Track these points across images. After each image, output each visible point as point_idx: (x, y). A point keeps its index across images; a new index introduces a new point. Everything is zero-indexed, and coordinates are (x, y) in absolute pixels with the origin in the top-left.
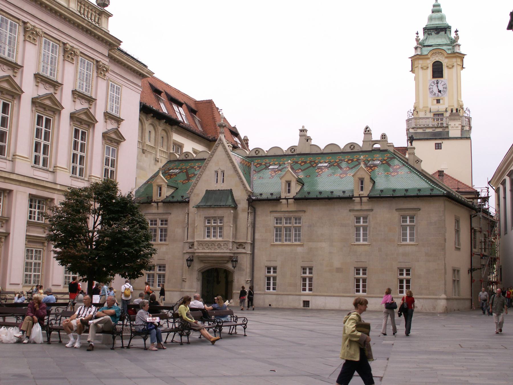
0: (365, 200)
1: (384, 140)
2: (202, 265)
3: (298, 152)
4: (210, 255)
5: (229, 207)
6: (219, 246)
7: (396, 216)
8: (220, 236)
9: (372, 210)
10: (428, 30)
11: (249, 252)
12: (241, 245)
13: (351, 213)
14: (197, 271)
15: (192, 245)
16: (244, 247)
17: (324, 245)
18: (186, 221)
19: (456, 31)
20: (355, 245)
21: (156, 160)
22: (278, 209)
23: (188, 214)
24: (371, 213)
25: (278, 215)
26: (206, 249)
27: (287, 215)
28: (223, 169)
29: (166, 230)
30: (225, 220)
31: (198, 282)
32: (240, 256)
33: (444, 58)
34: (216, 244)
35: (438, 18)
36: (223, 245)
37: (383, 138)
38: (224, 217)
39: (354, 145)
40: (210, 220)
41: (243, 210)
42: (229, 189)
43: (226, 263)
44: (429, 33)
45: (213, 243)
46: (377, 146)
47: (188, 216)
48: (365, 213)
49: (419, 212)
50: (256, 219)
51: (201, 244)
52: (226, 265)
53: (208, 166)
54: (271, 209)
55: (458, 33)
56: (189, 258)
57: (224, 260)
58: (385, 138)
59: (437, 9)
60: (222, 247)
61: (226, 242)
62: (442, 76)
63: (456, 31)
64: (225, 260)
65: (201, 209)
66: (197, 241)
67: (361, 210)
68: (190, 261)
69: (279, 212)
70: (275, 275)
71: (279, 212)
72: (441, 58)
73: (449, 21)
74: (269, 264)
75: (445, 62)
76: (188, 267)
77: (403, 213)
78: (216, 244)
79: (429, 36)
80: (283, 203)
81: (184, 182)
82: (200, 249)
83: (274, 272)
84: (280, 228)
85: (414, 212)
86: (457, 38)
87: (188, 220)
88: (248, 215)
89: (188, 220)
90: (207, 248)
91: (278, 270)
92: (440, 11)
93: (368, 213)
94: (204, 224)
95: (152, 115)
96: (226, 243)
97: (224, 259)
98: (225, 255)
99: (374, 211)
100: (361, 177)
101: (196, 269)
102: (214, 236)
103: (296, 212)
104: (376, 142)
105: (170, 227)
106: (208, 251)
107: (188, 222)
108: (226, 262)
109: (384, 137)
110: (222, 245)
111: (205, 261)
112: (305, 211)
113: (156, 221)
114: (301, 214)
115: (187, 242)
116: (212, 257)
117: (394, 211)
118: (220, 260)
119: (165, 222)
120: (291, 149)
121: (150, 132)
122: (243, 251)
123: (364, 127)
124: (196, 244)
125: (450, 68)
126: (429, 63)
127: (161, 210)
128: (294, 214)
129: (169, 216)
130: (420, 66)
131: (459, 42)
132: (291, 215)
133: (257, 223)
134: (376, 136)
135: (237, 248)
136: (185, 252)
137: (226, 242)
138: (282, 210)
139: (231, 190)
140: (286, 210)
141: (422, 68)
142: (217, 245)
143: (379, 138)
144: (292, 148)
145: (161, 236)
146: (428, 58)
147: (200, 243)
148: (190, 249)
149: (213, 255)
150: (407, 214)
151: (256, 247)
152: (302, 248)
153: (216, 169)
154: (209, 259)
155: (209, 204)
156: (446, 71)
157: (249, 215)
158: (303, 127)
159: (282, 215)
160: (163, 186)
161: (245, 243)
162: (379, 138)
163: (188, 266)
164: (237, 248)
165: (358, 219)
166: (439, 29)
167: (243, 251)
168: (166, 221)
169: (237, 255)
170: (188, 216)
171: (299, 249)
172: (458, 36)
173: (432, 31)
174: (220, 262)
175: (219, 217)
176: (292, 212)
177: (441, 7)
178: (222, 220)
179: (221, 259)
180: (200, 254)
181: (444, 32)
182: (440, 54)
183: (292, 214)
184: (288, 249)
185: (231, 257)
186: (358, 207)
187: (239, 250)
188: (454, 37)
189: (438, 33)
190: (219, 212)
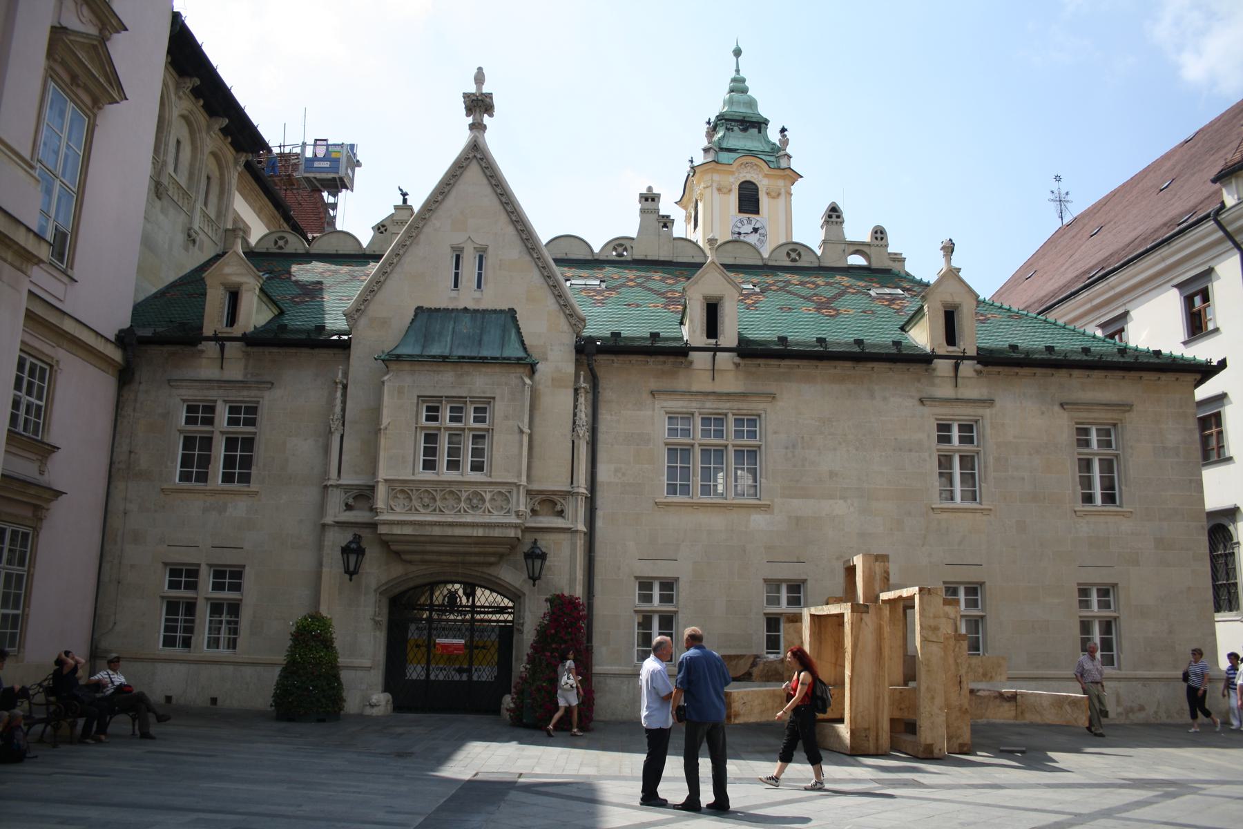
0: (967, 368)
1: (879, 242)
2: (397, 570)
3: (638, 254)
4: (437, 531)
5: (519, 362)
6: (476, 500)
7: (1062, 426)
8: (477, 467)
9: (989, 402)
10: (726, 120)
11: (581, 527)
12: (549, 502)
13: (926, 410)
14: (375, 591)
15: (364, 495)
16: (559, 508)
17: (839, 507)
18: (338, 409)
19: (783, 130)
20: (943, 510)
21: (189, 236)
22: (681, 384)
23: (345, 387)
24: (987, 412)
25: (677, 405)
26: (422, 510)
27: (710, 406)
28: (481, 240)
29: (249, 443)
30: (500, 408)
31: (378, 633)
32: (545, 542)
33: (760, 176)
34: (464, 496)
35: (744, 103)
36: (492, 499)
37: (876, 238)
38: (494, 398)
39: (800, 249)
40: (436, 409)
41: (557, 382)
42: (505, 307)
43: (491, 564)
44: (729, 126)
45: (451, 491)
46: (856, 260)
47: (344, 395)
48: (965, 413)
49: (1127, 415)
50: (600, 417)
51: (403, 491)
52: (493, 571)
53: (426, 230)
54: (653, 384)
55: (786, 133)
56: (350, 542)
57: (485, 554)
58: (882, 239)
59: (738, 86)
60: (487, 505)
61: (504, 489)
62: (757, 212)
63: (783, 130)
64: (494, 554)
65: (407, 367)
66: (386, 481)
67: (957, 400)
68: (353, 551)
69: (684, 393)
70: (668, 608)
71: (684, 393)
72: (756, 177)
73: (763, 111)
74: (648, 570)
75: (763, 184)
76: (347, 576)
77: (1083, 415)
78: (464, 496)
79: (727, 133)
80: (696, 365)
81: (297, 300)
82: (398, 510)
83: (666, 599)
84: (686, 451)
85: (1115, 416)
86: (785, 141)
87: (344, 410)
88: (576, 400)
89: (344, 410)
90: (426, 506)
91: (683, 592)
92: (744, 91)
93: (980, 411)
94: (417, 424)
95: (197, 81)
96: (504, 492)
97: (490, 549)
98: (497, 533)
99: (998, 404)
100: (949, 299)
101: (373, 585)
102: (453, 465)
103: (744, 396)
104: (859, 248)
105: (267, 433)
106: (429, 518)
107: (343, 416)
108: (492, 559)
109: (879, 235)
110: (488, 497)
111: (408, 557)
112: (772, 397)
113: (211, 409)
114: (761, 406)
115: (338, 486)
116: (444, 540)
117: (1057, 408)
118: (470, 554)
119: (245, 414)
120: (617, 242)
121: (178, 142)
122: (558, 522)
123: (823, 208)
124: (381, 491)
125: (773, 198)
126: (734, 182)
127: (235, 371)
128: (736, 405)
129: (267, 394)
130: (715, 185)
131: (789, 150)
132: (724, 406)
133: (602, 428)
134: (856, 230)
135: (534, 512)
136: (329, 520)
137: (504, 489)
138: (695, 388)
139: (512, 312)
140: (708, 387)
141: (719, 190)
142: (469, 499)
143: (866, 237)
144: (619, 244)
145: (229, 462)
146: (732, 173)
147: (401, 489)
148: (348, 513)
149: (449, 532)
150: (1095, 419)
151: (600, 514)
152: (768, 516)
153: (458, 239)
154: (429, 548)
155: (435, 350)
156: (764, 201)
157: (582, 400)
158: (650, 189)
159: (694, 405)
160: (244, 288)
161: (566, 494)
162: (866, 237)
163: (347, 571)
164: (534, 512)
165: (944, 428)
166: (749, 122)
167: (558, 522)
168: (252, 410)
169: (539, 536)
170: (344, 395)
171: (758, 521)
172: (788, 140)
173: (733, 124)
174: (474, 559)
175: (473, 399)
176: (729, 396)
177: (747, 83)
178: (484, 410)
179: (476, 550)
180: (397, 530)
181: (755, 131)
182: (755, 167)
183: (728, 405)
184: (717, 521)
185: (513, 544)
186: (946, 391)
187: (541, 518)
188: (780, 140)
189: (745, 130)
190: (479, 383)
